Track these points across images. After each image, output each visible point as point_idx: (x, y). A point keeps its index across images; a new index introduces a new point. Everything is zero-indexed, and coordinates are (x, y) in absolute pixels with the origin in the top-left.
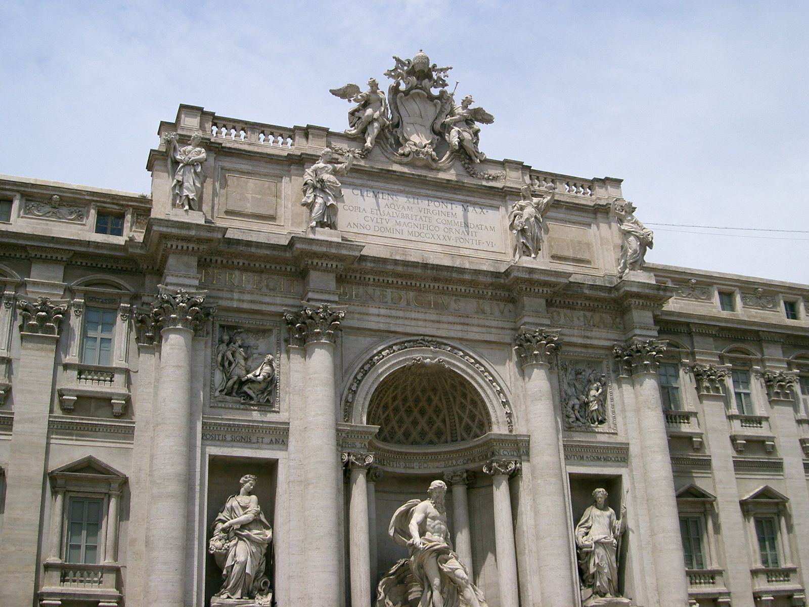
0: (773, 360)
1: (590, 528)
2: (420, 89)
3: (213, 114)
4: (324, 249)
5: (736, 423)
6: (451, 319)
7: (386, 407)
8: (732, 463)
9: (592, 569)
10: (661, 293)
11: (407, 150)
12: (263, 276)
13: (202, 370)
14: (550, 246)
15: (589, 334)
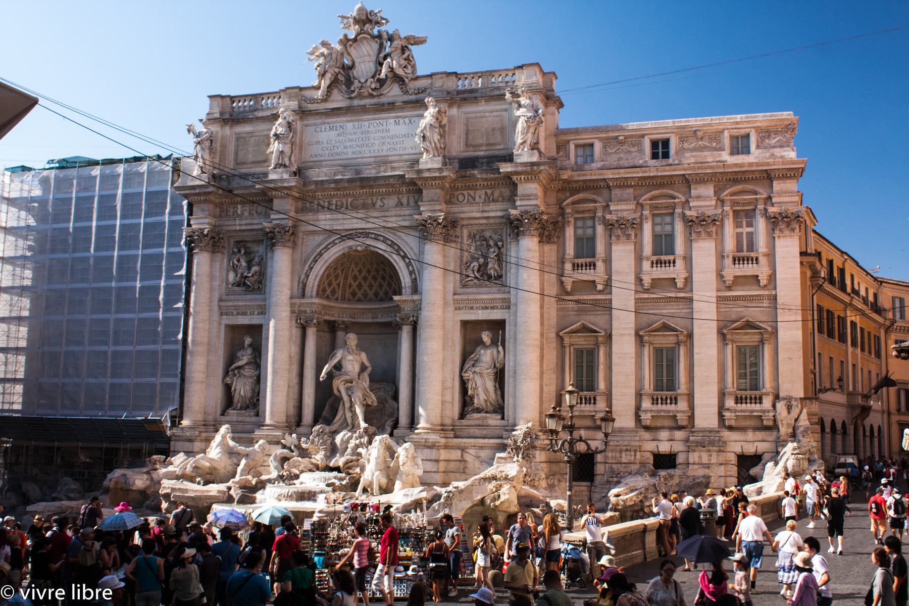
0: (698, 197)
1: (476, 361)
2: (365, 33)
3: (229, 96)
4: (272, 185)
5: (646, 265)
6: (376, 214)
7: (355, 278)
8: (633, 302)
9: (470, 392)
10: (535, 168)
11: (352, 89)
12: (256, 205)
13: (218, 274)
14: (467, 138)
15: (486, 208)
